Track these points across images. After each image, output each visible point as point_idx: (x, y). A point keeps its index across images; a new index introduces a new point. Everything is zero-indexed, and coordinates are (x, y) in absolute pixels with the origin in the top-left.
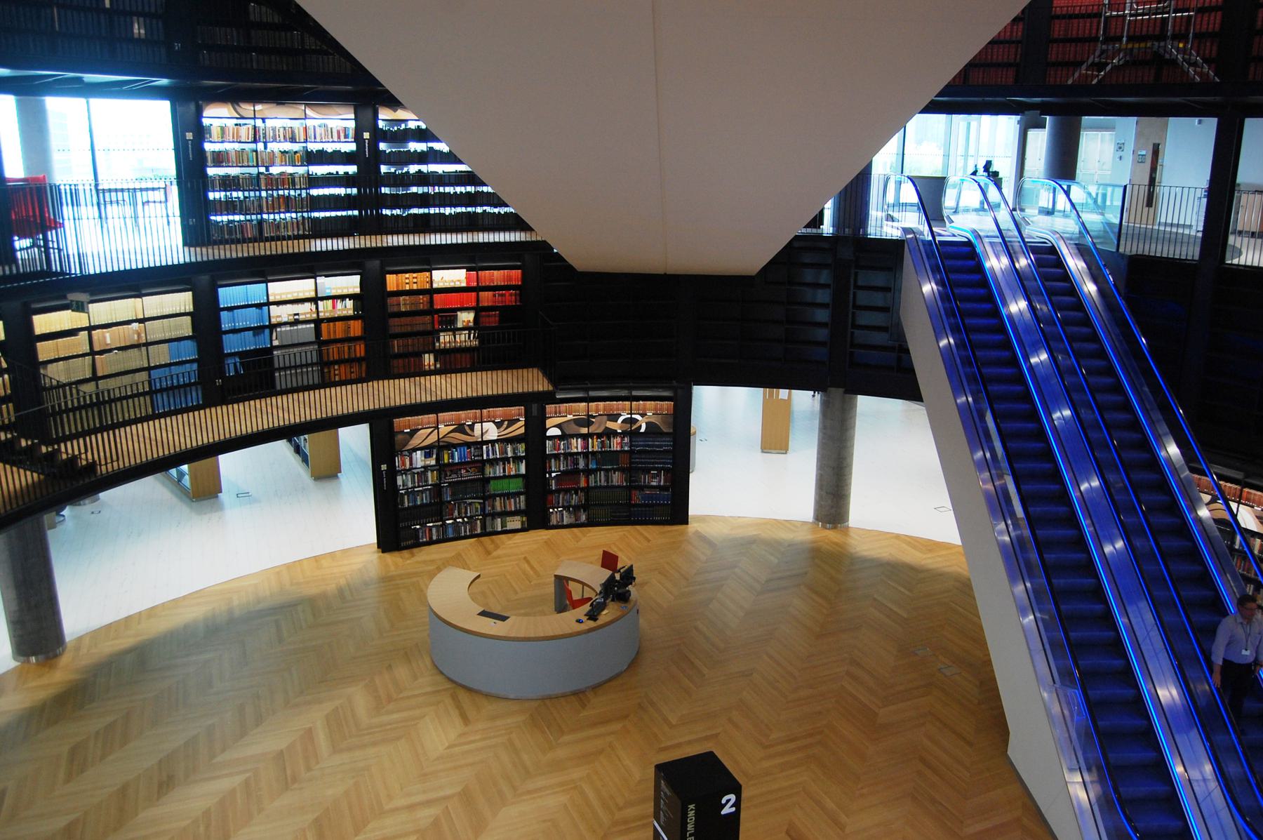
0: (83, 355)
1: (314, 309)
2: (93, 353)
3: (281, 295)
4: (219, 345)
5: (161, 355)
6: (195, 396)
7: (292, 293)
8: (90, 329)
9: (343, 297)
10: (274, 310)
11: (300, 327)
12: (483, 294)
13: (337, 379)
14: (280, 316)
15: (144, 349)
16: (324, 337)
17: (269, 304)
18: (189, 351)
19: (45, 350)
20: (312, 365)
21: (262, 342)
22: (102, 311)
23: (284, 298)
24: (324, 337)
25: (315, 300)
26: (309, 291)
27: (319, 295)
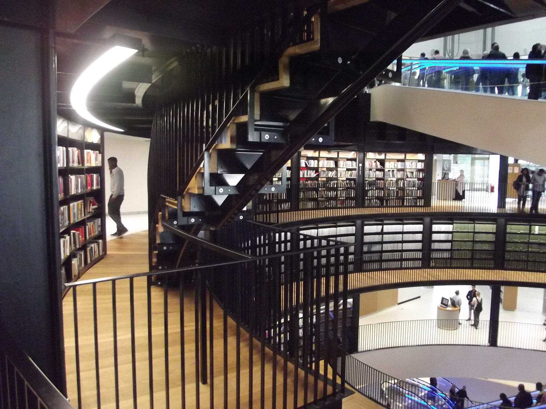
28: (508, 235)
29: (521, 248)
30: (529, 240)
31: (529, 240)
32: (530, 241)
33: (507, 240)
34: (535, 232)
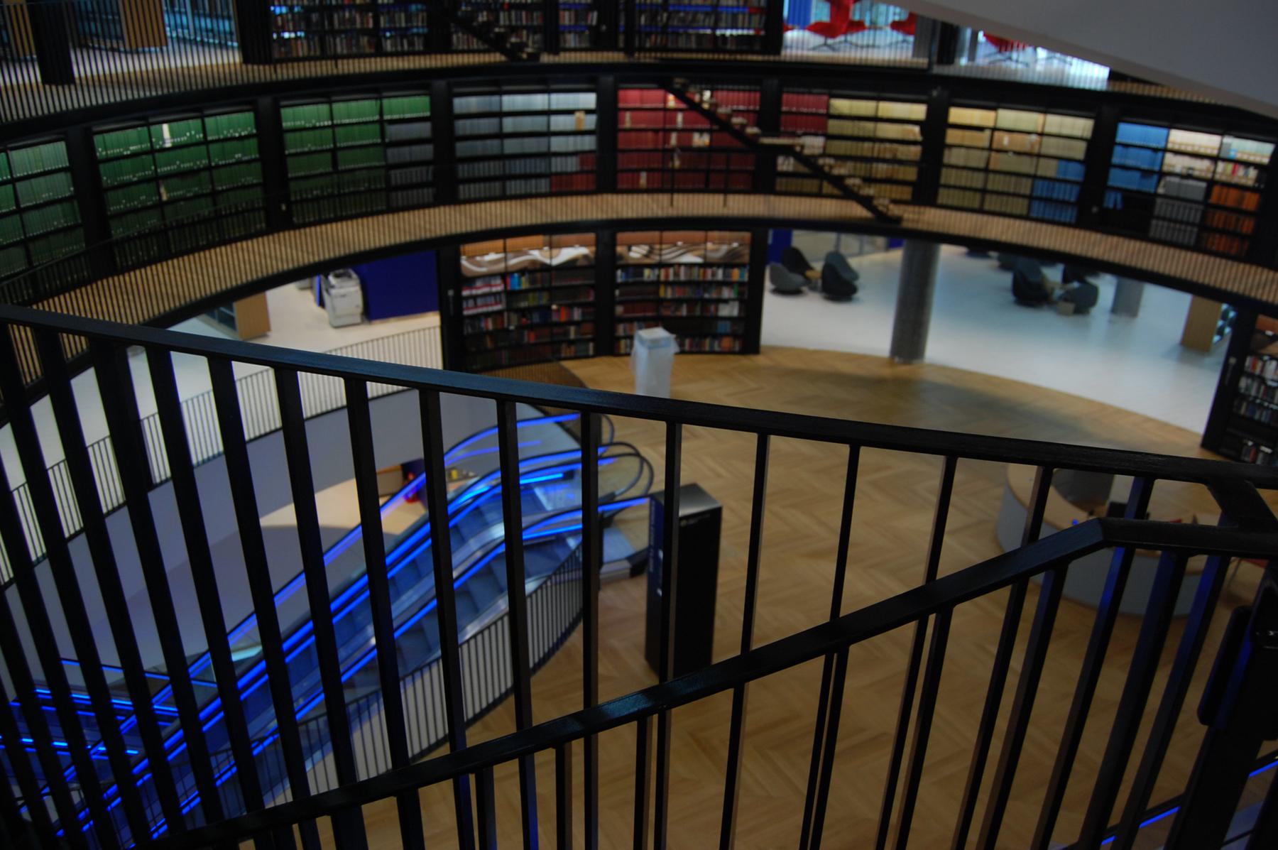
0: (983, 149)
1: (1212, 169)
2: (990, 149)
3: (1180, 144)
4: (1105, 176)
5: (1048, 169)
6: (1069, 214)
7: (1193, 146)
8: (994, 129)
9: (1247, 164)
10: (1169, 157)
11: (1191, 182)
12: (1221, 165)
13: (1214, 248)
14: (1173, 166)
15: (1035, 160)
16: (1213, 200)
17: (1165, 150)
18: (1076, 173)
19: (952, 136)
20: (1193, 224)
21: (1148, 186)
22: (1008, 117)
23: (1183, 148)
24: (1213, 200)
25: (1215, 159)
26: (1213, 149)
27: (1222, 155)
28: (103, 168)
29: (143, 197)
30: (156, 169)
31: (156, 169)
32: (159, 170)
33: (105, 185)
34: (164, 143)
